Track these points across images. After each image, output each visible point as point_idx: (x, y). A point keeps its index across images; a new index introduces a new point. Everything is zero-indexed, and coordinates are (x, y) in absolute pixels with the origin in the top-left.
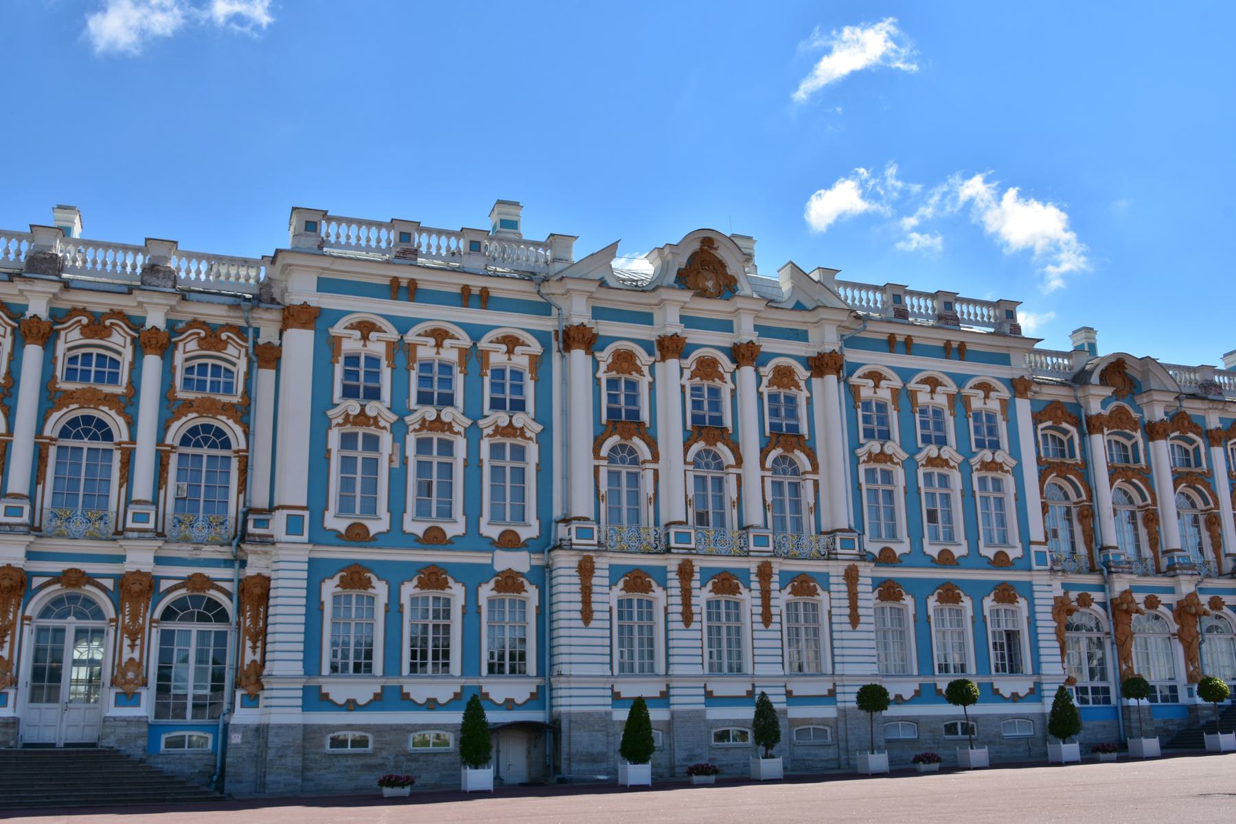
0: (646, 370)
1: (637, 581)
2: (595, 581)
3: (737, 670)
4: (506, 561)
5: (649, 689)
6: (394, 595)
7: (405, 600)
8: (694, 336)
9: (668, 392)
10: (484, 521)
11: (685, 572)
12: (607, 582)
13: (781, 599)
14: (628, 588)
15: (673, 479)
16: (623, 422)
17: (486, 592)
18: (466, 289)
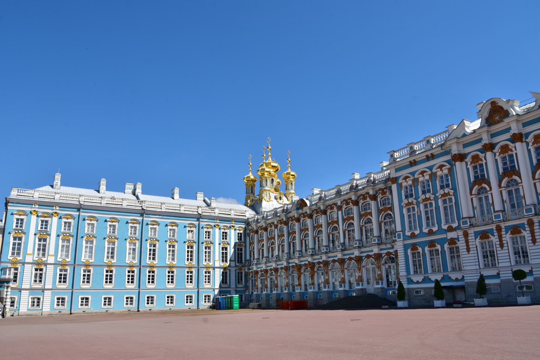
0: (483, 159)
1: (484, 235)
2: (469, 238)
3: (494, 265)
4: (451, 235)
5: (439, 277)
6: (423, 250)
7: (426, 252)
8: (496, 140)
9: (492, 164)
10: (443, 224)
11: (499, 229)
12: (474, 237)
13: (507, 237)
14: (481, 238)
15: (496, 195)
16: (480, 180)
17: (446, 246)
18: (427, 156)
